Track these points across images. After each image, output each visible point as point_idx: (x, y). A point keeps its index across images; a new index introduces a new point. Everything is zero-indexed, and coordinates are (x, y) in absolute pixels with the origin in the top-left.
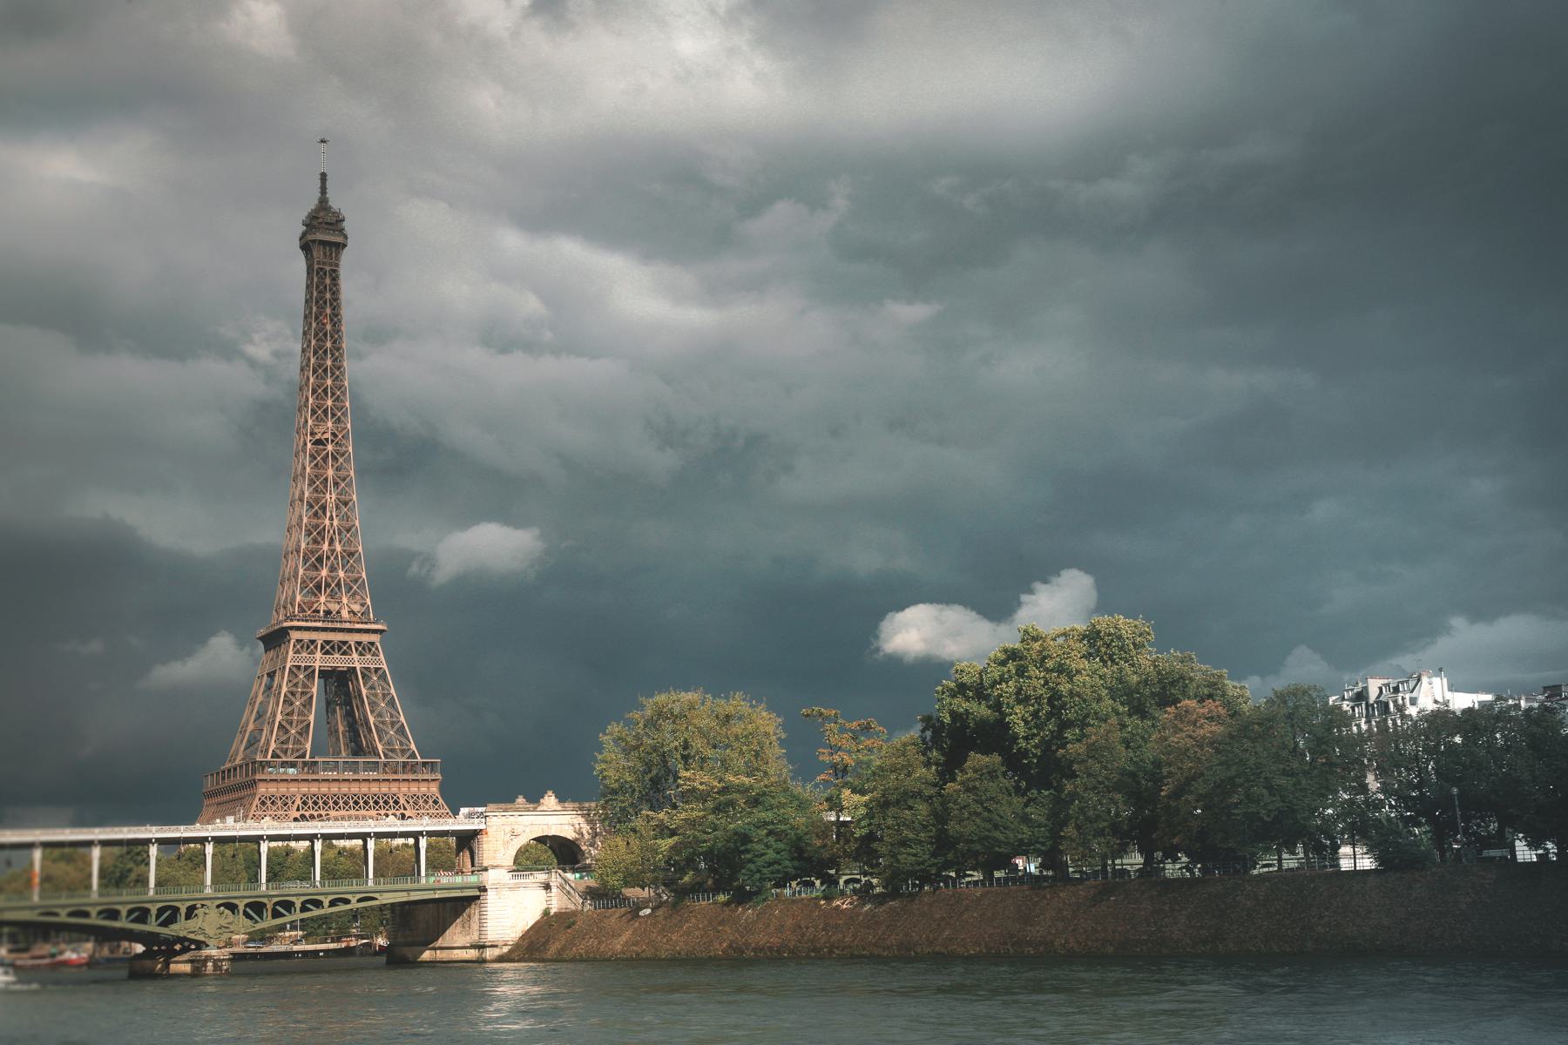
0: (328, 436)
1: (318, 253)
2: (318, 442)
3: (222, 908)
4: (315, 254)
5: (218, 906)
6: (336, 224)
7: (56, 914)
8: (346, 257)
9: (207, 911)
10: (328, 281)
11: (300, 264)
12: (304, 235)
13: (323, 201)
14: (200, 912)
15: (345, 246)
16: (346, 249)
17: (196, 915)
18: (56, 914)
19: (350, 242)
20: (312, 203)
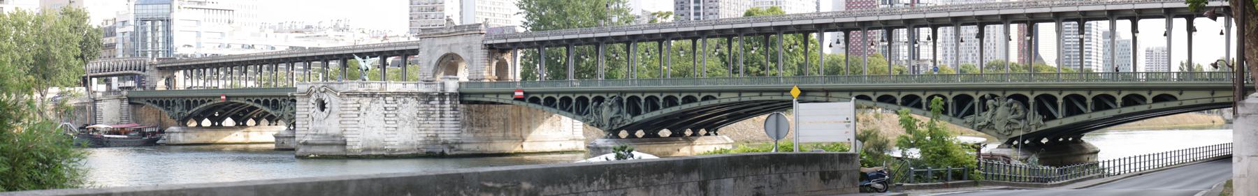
3: (1011, 100)
9: (997, 103)
14: (990, 102)
17: (988, 108)
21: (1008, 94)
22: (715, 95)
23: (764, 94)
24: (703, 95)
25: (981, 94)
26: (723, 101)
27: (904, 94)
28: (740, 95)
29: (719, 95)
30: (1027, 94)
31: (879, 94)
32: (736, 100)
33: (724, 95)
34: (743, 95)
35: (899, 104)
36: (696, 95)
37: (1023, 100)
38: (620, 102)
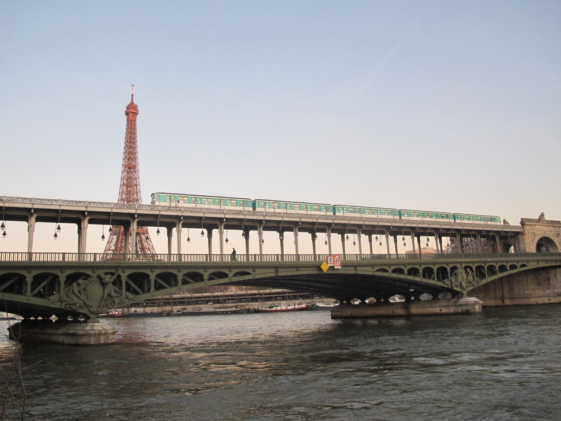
0: (133, 166)
1: (130, 115)
2: (130, 168)
4: (130, 116)
5: (465, 268)
6: (135, 107)
7: (386, 271)
8: (138, 117)
10: (133, 123)
11: (125, 117)
12: (126, 110)
13: (132, 102)
15: (138, 114)
16: (138, 115)
18: (386, 271)
19: (139, 113)
20: (129, 102)
21: (464, 265)
22: (250, 271)
23: (299, 269)
24: (235, 271)
25: (451, 266)
26: (257, 277)
27: (409, 267)
28: (277, 271)
29: (254, 271)
30: (471, 265)
31: (393, 268)
32: (274, 275)
33: (258, 271)
34: (280, 270)
35: (406, 274)
36: (226, 271)
37: (471, 268)
38: (117, 282)
